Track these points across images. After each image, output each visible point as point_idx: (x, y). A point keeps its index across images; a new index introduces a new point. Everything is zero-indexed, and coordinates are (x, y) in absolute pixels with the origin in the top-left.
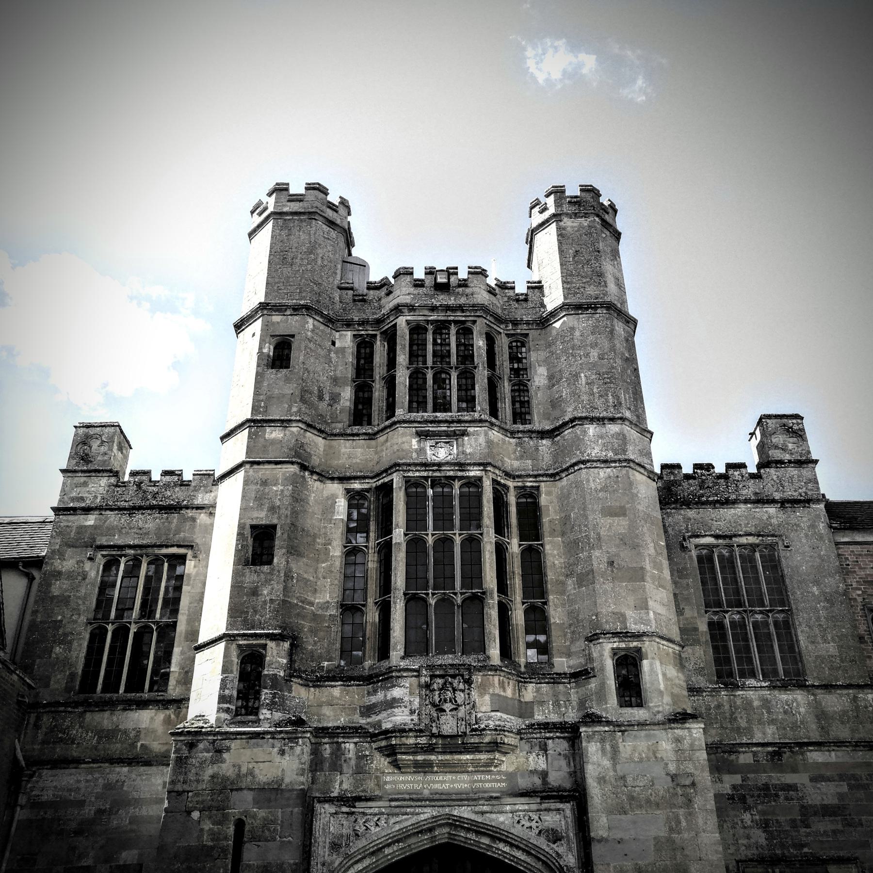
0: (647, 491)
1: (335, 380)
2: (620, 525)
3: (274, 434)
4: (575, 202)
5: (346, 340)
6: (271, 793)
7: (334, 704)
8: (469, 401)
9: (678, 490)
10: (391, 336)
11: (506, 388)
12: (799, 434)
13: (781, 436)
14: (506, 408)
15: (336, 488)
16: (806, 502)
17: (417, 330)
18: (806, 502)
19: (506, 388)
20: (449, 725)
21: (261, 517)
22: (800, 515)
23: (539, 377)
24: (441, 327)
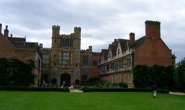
0: (79, 53)
1: (59, 43)
2: (77, 56)
3: (55, 48)
4: (78, 29)
5: (60, 40)
6: (56, 71)
7: (59, 66)
8: (68, 46)
9: (83, 52)
10: (63, 40)
11: (71, 43)
12: (92, 48)
13: (91, 47)
14: (71, 46)
15: (59, 52)
16: (91, 53)
17: (65, 40)
18: (91, 53)
19: (71, 45)
20: (66, 68)
21: (55, 54)
22: (90, 54)
23: (74, 44)
24: (67, 40)
